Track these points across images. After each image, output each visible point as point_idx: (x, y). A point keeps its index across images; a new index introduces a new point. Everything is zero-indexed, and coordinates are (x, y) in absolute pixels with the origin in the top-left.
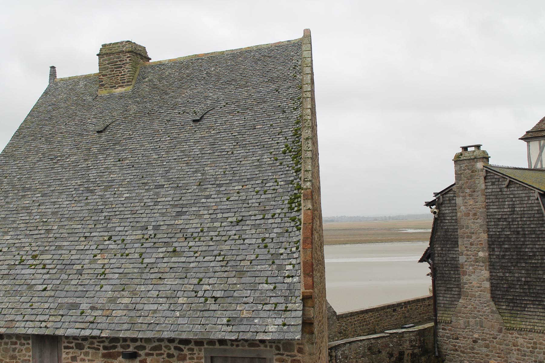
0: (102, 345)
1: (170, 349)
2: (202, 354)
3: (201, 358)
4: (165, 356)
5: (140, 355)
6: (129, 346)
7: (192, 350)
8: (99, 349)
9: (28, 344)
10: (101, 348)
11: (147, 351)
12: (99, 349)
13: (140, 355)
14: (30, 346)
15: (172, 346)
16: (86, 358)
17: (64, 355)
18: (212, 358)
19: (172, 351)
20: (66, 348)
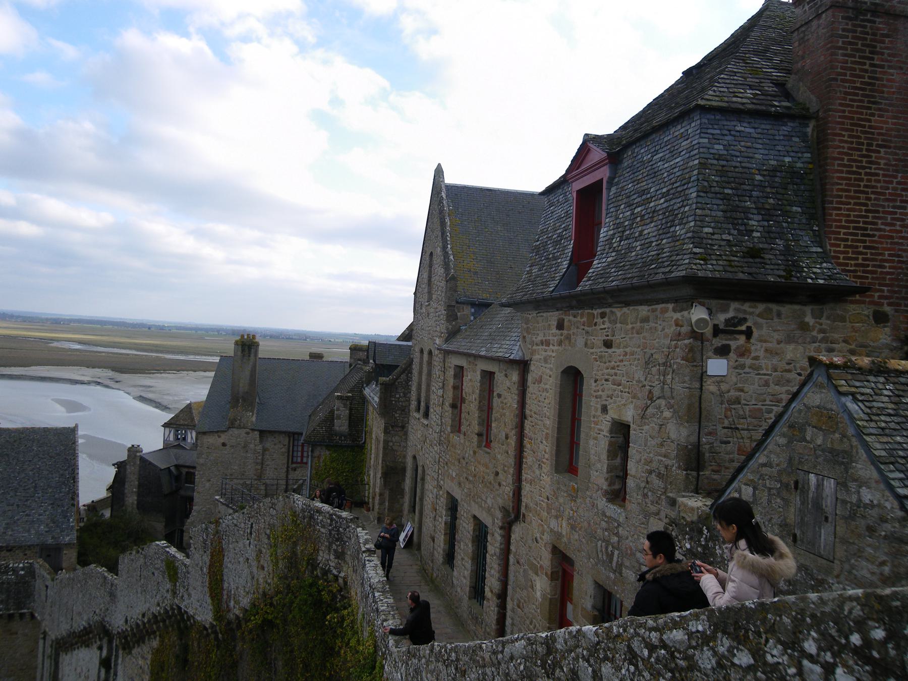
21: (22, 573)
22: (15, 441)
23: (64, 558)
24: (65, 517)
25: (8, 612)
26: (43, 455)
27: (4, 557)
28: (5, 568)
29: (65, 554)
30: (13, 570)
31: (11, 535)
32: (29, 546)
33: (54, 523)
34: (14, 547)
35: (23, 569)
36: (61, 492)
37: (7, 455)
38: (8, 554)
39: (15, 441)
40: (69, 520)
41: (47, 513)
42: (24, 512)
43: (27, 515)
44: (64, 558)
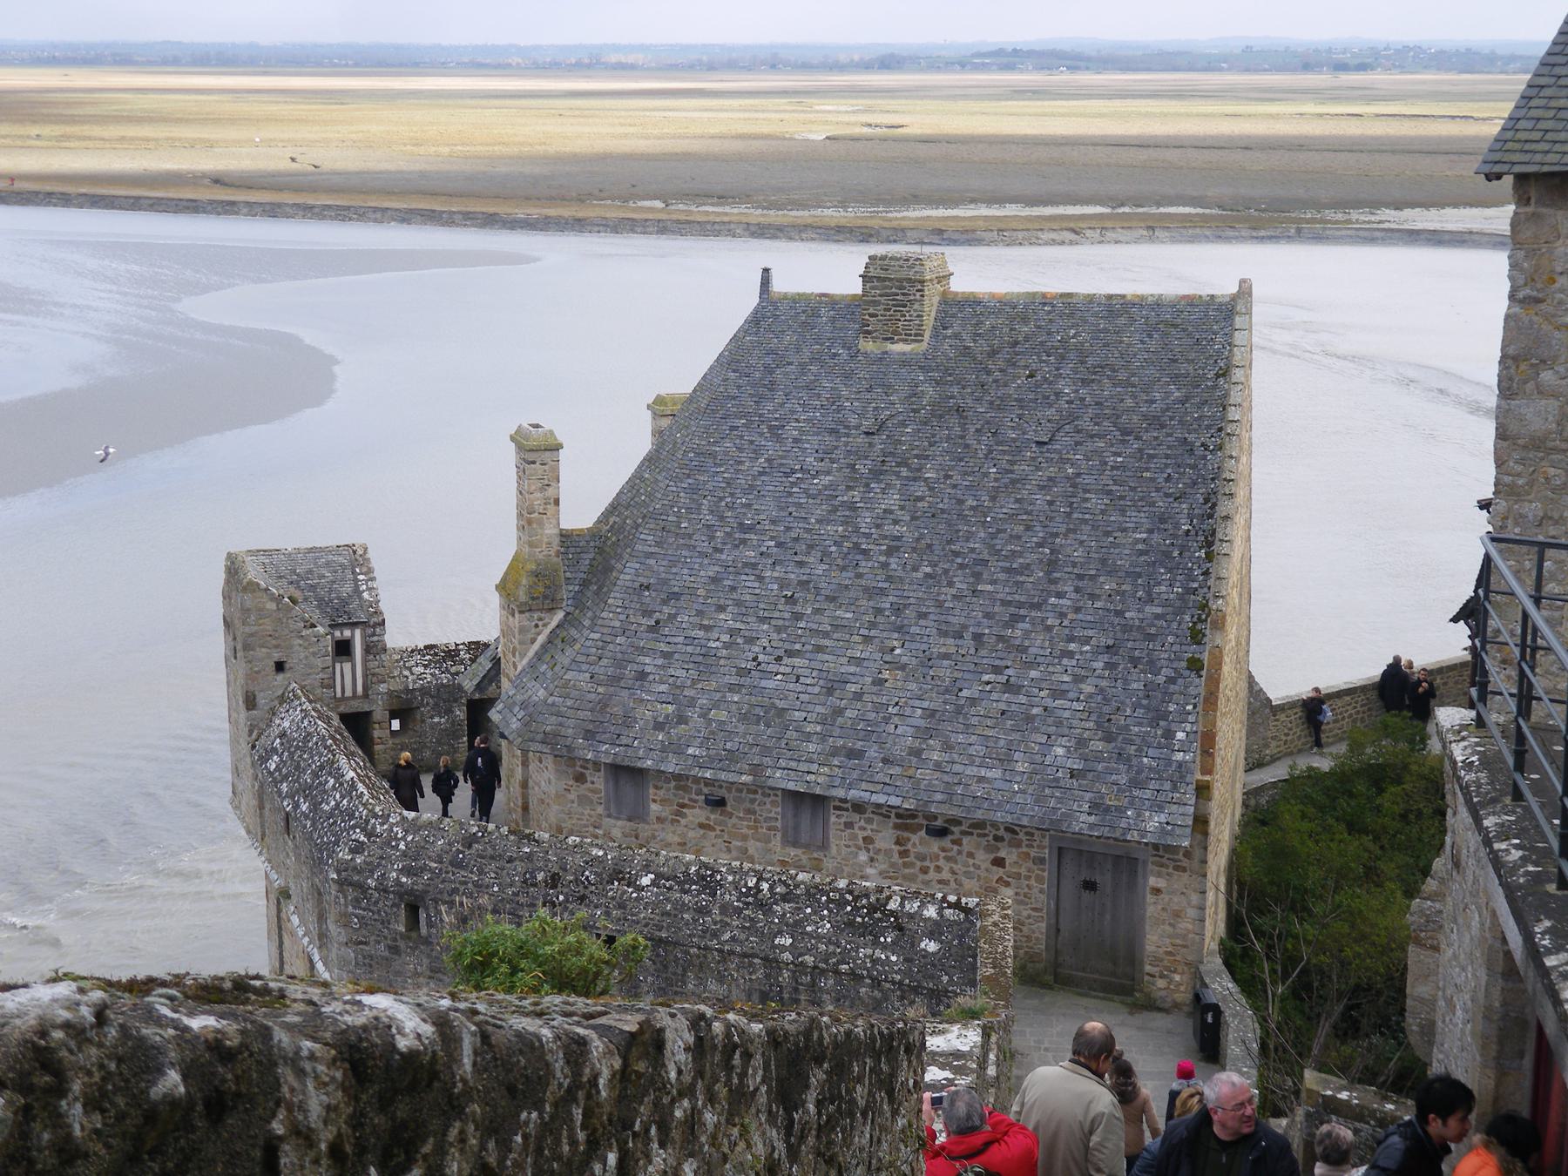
0: (894, 811)
2: (1046, 842)
3: (1044, 847)
4: (991, 838)
5: (952, 833)
7: (1032, 835)
8: (889, 817)
9: (776, 795)
10: (893, 815)
12: (889, 817)
13: (952, 833)
14: (779, 799)
16: (869, 827)
17: (833, 819)
18: (1060, 849)
19: (1002, 832)
20: (836, 808)
21: (932, 947)
22: (993, 353)
23: (1152, 908)
24: (1158, 717)
26: (1096, 419)
27: (922, 858)
28: (872, 909)
29: (1157, 891)
30: (900, 928)
31: (938, 766)
33: (1108, 738)
34: (957, 822)
35: (935, 930)
36: (1150, 600)
37: (959, 410)
38: (935, 845)
39: (993, 353)
40: (1169, 735)
41: (1088, 688)
42: (997, 670)
43: (1008, 687)
44: (1151, 910)
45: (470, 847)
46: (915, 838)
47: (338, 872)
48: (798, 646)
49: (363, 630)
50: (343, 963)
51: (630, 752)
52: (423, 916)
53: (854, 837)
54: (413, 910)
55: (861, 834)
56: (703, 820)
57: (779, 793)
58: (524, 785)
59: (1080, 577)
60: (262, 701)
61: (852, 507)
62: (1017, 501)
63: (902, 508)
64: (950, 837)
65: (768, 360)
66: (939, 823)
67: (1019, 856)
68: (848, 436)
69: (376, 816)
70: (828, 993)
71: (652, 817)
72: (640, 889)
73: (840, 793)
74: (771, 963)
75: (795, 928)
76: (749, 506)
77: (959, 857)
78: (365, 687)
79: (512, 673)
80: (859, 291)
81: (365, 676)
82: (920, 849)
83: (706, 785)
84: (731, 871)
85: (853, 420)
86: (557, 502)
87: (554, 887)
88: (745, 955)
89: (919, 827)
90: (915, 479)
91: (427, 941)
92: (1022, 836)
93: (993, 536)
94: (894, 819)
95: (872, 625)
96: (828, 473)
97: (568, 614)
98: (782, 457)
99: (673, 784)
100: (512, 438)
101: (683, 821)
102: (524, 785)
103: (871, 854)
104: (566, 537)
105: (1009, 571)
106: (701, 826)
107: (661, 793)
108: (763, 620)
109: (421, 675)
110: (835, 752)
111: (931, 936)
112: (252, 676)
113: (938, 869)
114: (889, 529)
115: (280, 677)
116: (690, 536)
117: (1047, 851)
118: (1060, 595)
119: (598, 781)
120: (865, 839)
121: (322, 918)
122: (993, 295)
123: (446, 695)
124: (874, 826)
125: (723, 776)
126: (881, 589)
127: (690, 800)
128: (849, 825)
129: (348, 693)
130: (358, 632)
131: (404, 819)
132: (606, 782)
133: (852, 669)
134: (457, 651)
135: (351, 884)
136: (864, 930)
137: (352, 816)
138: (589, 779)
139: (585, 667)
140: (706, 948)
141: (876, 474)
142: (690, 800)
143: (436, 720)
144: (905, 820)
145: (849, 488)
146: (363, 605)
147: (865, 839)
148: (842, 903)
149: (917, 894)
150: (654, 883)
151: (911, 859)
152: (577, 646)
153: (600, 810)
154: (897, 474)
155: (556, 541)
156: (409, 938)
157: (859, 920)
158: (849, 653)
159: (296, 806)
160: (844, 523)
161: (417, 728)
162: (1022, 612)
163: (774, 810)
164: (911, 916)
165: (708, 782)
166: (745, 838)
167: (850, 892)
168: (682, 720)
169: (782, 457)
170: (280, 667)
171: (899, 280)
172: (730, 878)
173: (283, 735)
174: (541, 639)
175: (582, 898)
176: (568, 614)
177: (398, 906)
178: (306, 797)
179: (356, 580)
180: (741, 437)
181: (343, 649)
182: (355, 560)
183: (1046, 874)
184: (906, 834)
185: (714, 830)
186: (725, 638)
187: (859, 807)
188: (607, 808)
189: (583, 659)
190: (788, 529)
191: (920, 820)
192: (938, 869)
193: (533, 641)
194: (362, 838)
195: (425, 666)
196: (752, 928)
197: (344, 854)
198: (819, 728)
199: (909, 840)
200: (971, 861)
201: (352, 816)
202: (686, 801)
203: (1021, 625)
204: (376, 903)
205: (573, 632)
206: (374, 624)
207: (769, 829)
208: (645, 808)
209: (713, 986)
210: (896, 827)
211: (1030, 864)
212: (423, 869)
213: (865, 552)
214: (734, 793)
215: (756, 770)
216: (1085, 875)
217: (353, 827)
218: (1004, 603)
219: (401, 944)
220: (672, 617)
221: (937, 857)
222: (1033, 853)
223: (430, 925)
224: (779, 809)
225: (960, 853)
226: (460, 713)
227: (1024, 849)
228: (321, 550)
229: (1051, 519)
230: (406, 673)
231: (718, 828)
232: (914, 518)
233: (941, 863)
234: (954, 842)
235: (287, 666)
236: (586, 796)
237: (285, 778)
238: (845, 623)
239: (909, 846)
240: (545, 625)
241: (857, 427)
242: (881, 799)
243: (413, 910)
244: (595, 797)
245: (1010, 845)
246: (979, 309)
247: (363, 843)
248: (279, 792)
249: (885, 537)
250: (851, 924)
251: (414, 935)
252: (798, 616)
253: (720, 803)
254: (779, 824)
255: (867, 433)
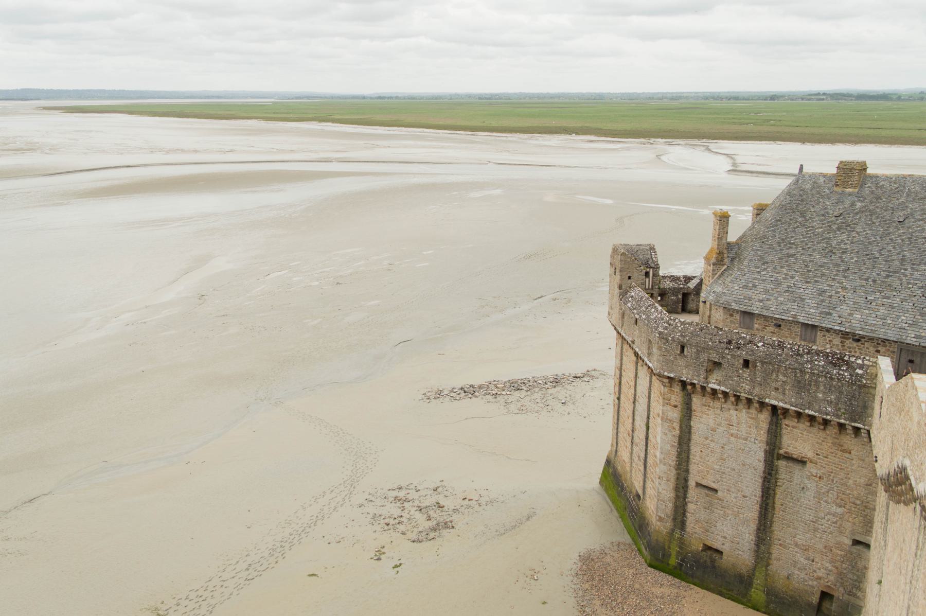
0: (841, 333)
1: (879, 341)
2: (896, 346)
5: (862, 341)
6: (856, 336)
11: (866, 339)
12: (839, 334)
13: (862, 341)
14: (800, 326)
15: (880, 340)
16: (831, 337)
17: (819, 333)
18: (901, 349)
19: (880, 342)
20: (820, 330)
25: (838, 420)
27: (850, 348)
28: (838, 359)
32: (884, 341)
35: (861, 367)
38: (855, 344)
45: (702, 330)
46: (847, 342)
47: (659, 334)
48: (809, 280)
49: (653, 270)
50: (658, 361)
51: (752, 308)
52: (685, 349)
53: (826, 340)
54: (683, 348)
55: (828, 339)
56: (772, 331)
57: (800, 324)
58: (709, 317)
59: (914, 264)
60: (623, 287)
61: (829, 239)
62: (890, 239)
63: (848, 240)
64: (860, 342)
65: (801, 193)
66: (857, 337)
67: (886, 350)
68: (828, 217)
69: (671, 320)
70: (822, 383)
71: (755, 328)
72: (758, 347)
73: (823, 325)
74: (803, 372)
75: (811, 362)
76: (792, 237)
77: (863, 349)
78: (652, 286)
79: (708, 283)
80: (835, 172)
81: (652, 283)
82: (849, 345)
83: (775, 320)
84: (789, 344)
85: (831, 212)
86: (727, 233)
87: (730, 344)
88: (793, 369)
89: (850, 338)
90: (853, 231)
91: (686, 357)
92: (887, 343)
93: (881, 250)
94: (840, 335)
95: (837, 275)
96: (822, 228)
97: (728, 267)
98: (805, 222)
99: (763, 319)
100: (713, 213)
101: (765, 331)
102: (709, 317)
103: (831, 345)
104: (729, 243)
105: (886, 261)
106: (772, 332)
107: (759, 321)
108: (797, 272)
109: (668, 284)
110: (821, 313)
111: (860, 369)
112: (622, 280)
113: (855, 352)
114: (843, 246)
115: (629, 281)
116: (772, 245)
117: (896, 349)
118: (905, 270)
119: (737, 317)
120: (829, 340)
121: (649, 348)
122: (883, 175)
123: (675, 291)
124: (833, 337)
125: (783, 317)
126: (839, 264)
127: (769, 324)
128: (824, 336)
129: (647, 287)
130: (651, 270)
131: (680, 321)
132: (740, 317)
133: (828, 288)
134: (680, 278)
135: (663, 338)
136: (835, 365)
137: (663, 319)
138: (734, 315)
139: (735, 282)
140: (780, 366)
141: (839, 229)
142: (769, 324)
143: (672, 298)
144: (845, 335)
145: (828, 233)
146: (653, 262)
147: (829, 340)
148: (828, 356)
149: (854, 356)
150: (763, 346)
151: (846, 348)
152: (733, 276)
153: (737, 325)
154: (846, 229)
155: (725, 244)
156: (681, 355)
157: (834, 362)
158: (827, 283)
159: (641, 316)
160: (826, 244)
161: (667, 299)
162: (891, 274)
163: (797, 329)
164: (853, 362)
165: (776, 319)
166: (787, 337)
167: (831, 353)
168: (768, 300)
169: (805, 222)
170: (629, 278)
171: (850, 169)
172: (789, 346)
173: (632, 297)
174: (718, 274)
175: (739, 348)
176: (728, 267)
177: (678, 346)
178: (644, 314)
179: (651, 255)
180: (791, 216)
181: (647, 274)
182: (652, 249)
183: (895, 356)
184: (845, 340)
185: (776, 334)
186: (784, 276)
187: (828, 330)
188: (740, 325)
189: (735, 280)
190: (807, 244)
191: (850, 336)
192: (855, 352)
193: (716, 274)
194: (667, 325)
195: (670, 282)
196: (797, 361)
197: (661, 329)
198: (816, 305)
199: (845, 342)
200: (868, 350)
201: (663, 319)
202: (767, 325)
203: (890, 278)
204: (671, 345)
205: (731, 272)
206: (657, 267)
207: (796, 335)
208: (753, 326)
209: (781, 377)
210: (841, 337)
211: (890, 353)
212: (686, 336)
213: (834, 253)
214: (784, 323)
215: (795, 316)
216: (910, 358)
217: (664, 322)
218: (884, 271)
219: (678, 357)
220: (765, 269)
221: (855, 348)
222: (891, 349)
223: (688, 352)
224: (800, 329)
225: (864, 347)
226: (680, 296)
227: (888, 348)
228: (641, 245)
229: (903, 246)
230: (664, 283)
231: (778, 333)
232: (852, 243)
233: (857, 350)
234: (861, 344)
235: (632, 278)
236: (733, 321)
237: (635, 309)
238: (826, 274)
239: (845, 344)
240: (720, 269)
241: (832, 214)
242: (838, 328)
243: (683, 348)
244: (736, 321)
245: (883, 346)
246: (878, 179)
247: (667, 327)
248: (633, 313)
249: (841, 248)
250: (831, 362)
251: (682, 354)
252: (809, 271)
253: (780, 326)
254: (799, 334)
255: (836, 216)
